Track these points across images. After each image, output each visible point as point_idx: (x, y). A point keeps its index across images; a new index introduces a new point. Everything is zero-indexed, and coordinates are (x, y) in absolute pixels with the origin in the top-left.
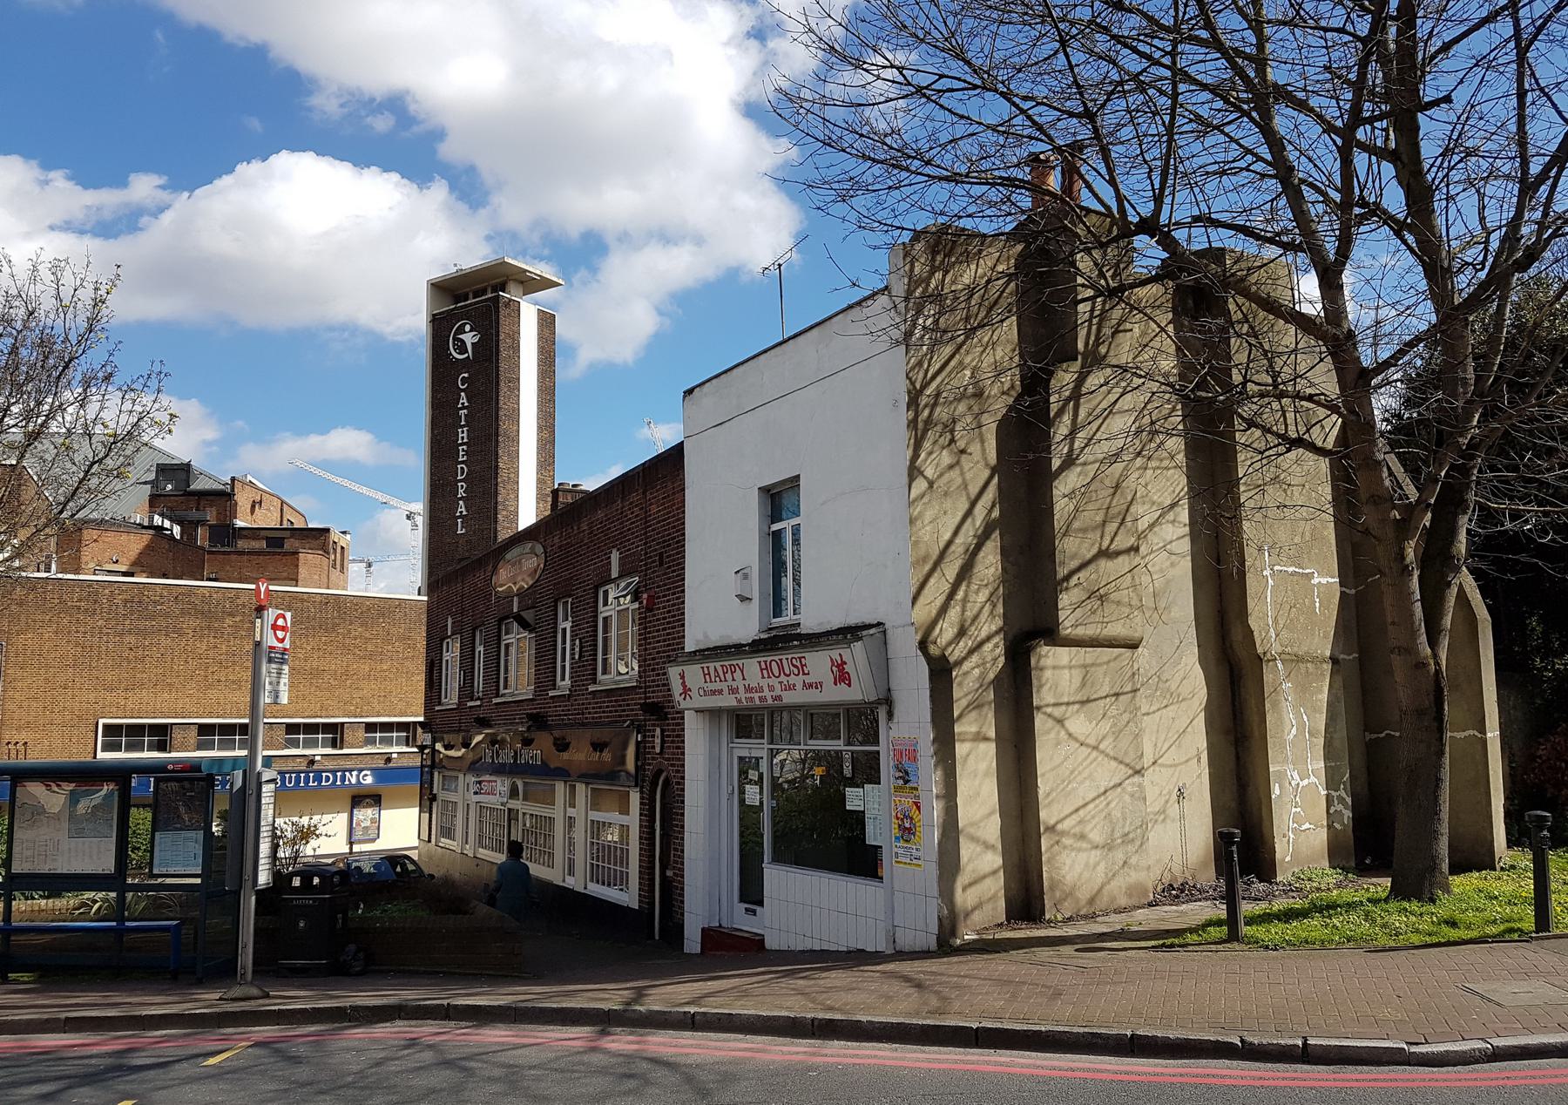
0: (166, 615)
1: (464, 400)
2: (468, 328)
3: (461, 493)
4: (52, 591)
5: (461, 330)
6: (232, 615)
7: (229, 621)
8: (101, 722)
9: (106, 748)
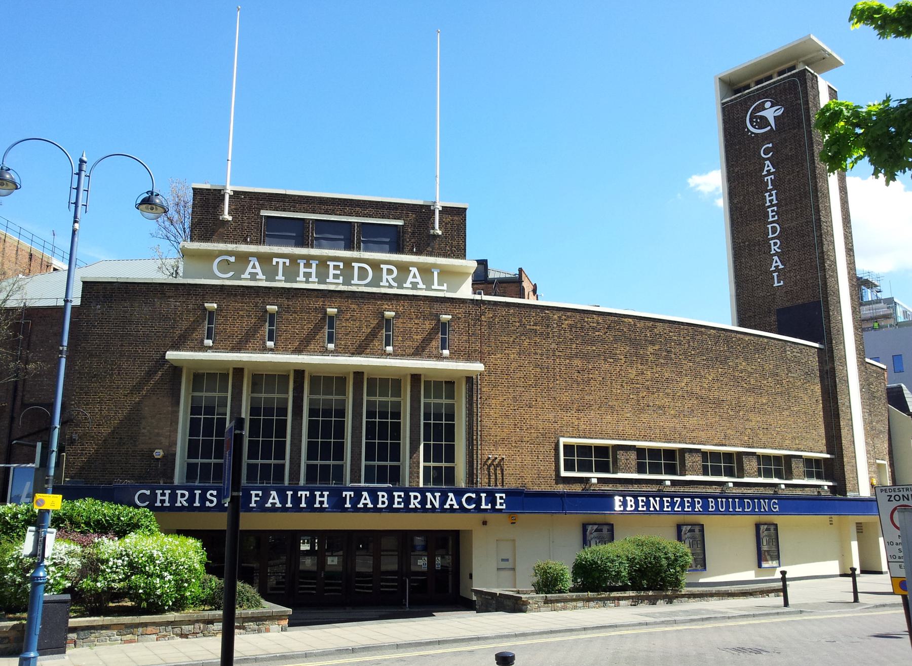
0: (603, 342)
1: (768, 166)
2: (768, 105)
3: (774, 249)
4: (513, 315)
5: (762, 108)
7: (650, 349)
8: (563, 441)
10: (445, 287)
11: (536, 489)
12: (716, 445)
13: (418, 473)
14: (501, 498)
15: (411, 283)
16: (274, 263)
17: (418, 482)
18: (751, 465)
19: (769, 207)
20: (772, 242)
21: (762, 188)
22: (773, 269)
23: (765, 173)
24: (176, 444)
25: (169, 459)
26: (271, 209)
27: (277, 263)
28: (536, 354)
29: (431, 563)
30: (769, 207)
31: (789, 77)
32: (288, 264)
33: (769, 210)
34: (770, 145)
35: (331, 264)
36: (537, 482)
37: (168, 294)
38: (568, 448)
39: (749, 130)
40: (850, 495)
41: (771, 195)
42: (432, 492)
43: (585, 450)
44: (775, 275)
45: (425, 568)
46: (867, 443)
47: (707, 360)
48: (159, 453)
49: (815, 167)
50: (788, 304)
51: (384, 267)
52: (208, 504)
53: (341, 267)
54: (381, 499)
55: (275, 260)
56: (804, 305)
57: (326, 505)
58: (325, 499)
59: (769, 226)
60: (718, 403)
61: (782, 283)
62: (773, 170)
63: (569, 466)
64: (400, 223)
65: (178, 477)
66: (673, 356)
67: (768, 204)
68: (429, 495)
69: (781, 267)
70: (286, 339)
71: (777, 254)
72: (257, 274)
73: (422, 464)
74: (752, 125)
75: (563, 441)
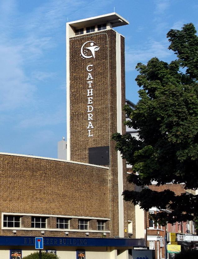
2: (92, 44)
3: (90, 118)
9: (4, 226)
20: (89, 115)
21: (86, 87)
22: (88, 128)
23: (88, 79)
30: (89, 96)
31: (103, 32)
33: (89, 98)
34: (92, 65)
38: (5, 216)
39: (82, 56)
44: (89, 131)
46: (124, 213)
50: (94, 146)
56: (101, 147)
59: (88, 106)
60: (64, 196)
62: (92, 78)
63: (5, 225)
67: (88, 95)
74: (83, 51)
75: (3, 214)
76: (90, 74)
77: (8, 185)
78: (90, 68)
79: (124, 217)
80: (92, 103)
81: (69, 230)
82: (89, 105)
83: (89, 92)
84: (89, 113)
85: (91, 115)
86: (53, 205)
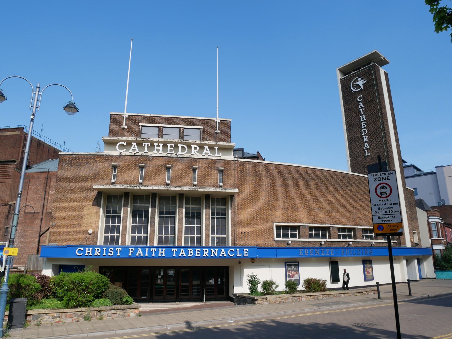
2: (359, 79)
3: (365, 140)
5: (357, 80)
6: (315, 180)
7: (314, 182)
9: (277, 237)
10: (221, 155)
11: (263, 246)
12: (344, 225)
13: (209, 240)
14: (246, 250)
15: (205, 153)
16: (143, 145)
17: (209, 244)
18: (359, 234)
19: (362, 122)
20: (364, 137)
22: (365, 148)
23: (360, 108)
24: (98, 227)
25: (95, 234)
26: (144, 123)
27: (145, 145)
28: (263, 185)
29: (216, 281)
30: (362, 122)
32: (149, 145)
33: (362, 123)
34: (361, 96)
35: (169, 145)
36: (264, 243)
37: (96, 159)
38: (278, 228)
40: (402, 246)
41: (363, 117)
42: (214, 248)
43: (285, 228)
44: (366, 151)
45: (213, 283)
46: (409, 224)
47: (339, 187)
48: (90, 231)
49: (381, 104)
50: (372, 163)
51: (193, 146)
52: (109, 254)
53: (173, 146)
54: (190, 252)
55: (144, 144)
57: (164, 255)
58: (164, 252)
59: (363, 130)
60: (344, 206)
61: (369, 154)
62: (363, 106)
63: (278, 236)
64: (202, 127)
65: (100, 241)
66: (324, 185)
67: (362, 120)
68: (212, 250)
69: (368, 147)
70: (148, 179)
71: (366, 142)
72: (136, 150)
73: (210, 236)
75: (275, 224)
76: (360, 103)
77: (280, 195)
78: (360, 98)
79: (409, 227)
80: (365, 126)
81: (353, 240)
82: (364, 128)
83: (361, 118)
84: (364, 135)
85: (366, 137)
86: (332, 215)
